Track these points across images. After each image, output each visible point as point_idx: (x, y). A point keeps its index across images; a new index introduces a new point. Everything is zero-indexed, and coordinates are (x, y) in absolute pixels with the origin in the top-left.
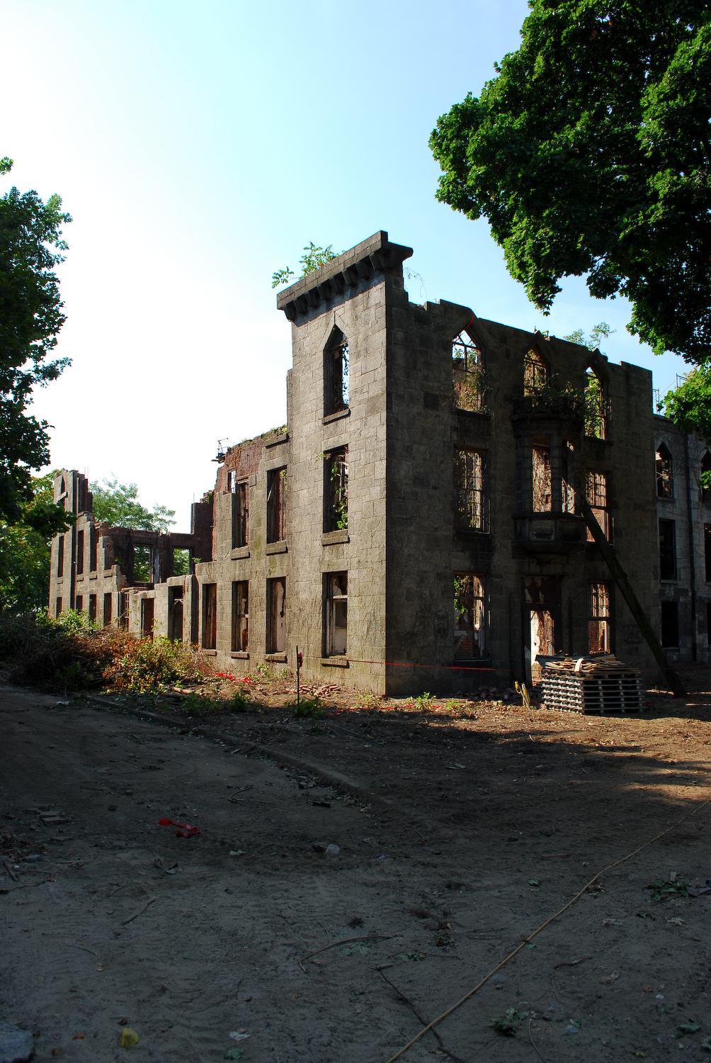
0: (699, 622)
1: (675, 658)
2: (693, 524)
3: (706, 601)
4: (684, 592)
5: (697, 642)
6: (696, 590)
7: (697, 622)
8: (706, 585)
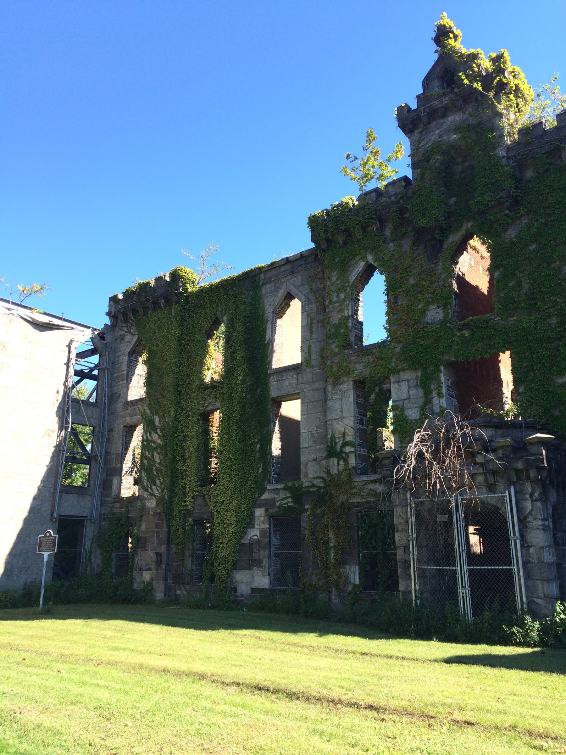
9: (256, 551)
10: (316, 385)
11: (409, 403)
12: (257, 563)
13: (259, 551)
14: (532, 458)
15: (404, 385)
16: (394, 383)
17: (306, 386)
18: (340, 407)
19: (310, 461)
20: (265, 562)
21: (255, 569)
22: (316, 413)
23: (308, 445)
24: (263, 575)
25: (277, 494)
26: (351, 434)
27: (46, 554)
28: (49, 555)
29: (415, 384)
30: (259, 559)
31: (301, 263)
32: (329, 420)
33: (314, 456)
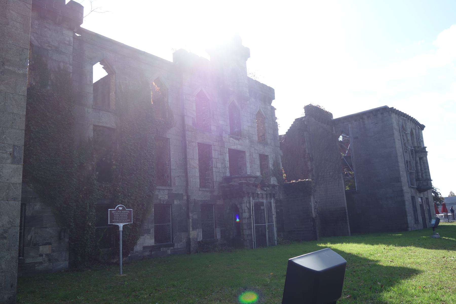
0: (192, 220)
1: (169, 252)
2: (187, 142)
5: (191, 237)
6: (189, 194)
7: (191, 220)
8: (199, 190)
9: (146, 224)
12: (148, 232)
14: (276, 191)
16: (213, 150)
20: (152, 231)
21: (146, 235)
23: (175, 168)
24: (151, 238)
27: (121, 225)
28: (124, 226)
30: (148, 229)
32: (188, 158)
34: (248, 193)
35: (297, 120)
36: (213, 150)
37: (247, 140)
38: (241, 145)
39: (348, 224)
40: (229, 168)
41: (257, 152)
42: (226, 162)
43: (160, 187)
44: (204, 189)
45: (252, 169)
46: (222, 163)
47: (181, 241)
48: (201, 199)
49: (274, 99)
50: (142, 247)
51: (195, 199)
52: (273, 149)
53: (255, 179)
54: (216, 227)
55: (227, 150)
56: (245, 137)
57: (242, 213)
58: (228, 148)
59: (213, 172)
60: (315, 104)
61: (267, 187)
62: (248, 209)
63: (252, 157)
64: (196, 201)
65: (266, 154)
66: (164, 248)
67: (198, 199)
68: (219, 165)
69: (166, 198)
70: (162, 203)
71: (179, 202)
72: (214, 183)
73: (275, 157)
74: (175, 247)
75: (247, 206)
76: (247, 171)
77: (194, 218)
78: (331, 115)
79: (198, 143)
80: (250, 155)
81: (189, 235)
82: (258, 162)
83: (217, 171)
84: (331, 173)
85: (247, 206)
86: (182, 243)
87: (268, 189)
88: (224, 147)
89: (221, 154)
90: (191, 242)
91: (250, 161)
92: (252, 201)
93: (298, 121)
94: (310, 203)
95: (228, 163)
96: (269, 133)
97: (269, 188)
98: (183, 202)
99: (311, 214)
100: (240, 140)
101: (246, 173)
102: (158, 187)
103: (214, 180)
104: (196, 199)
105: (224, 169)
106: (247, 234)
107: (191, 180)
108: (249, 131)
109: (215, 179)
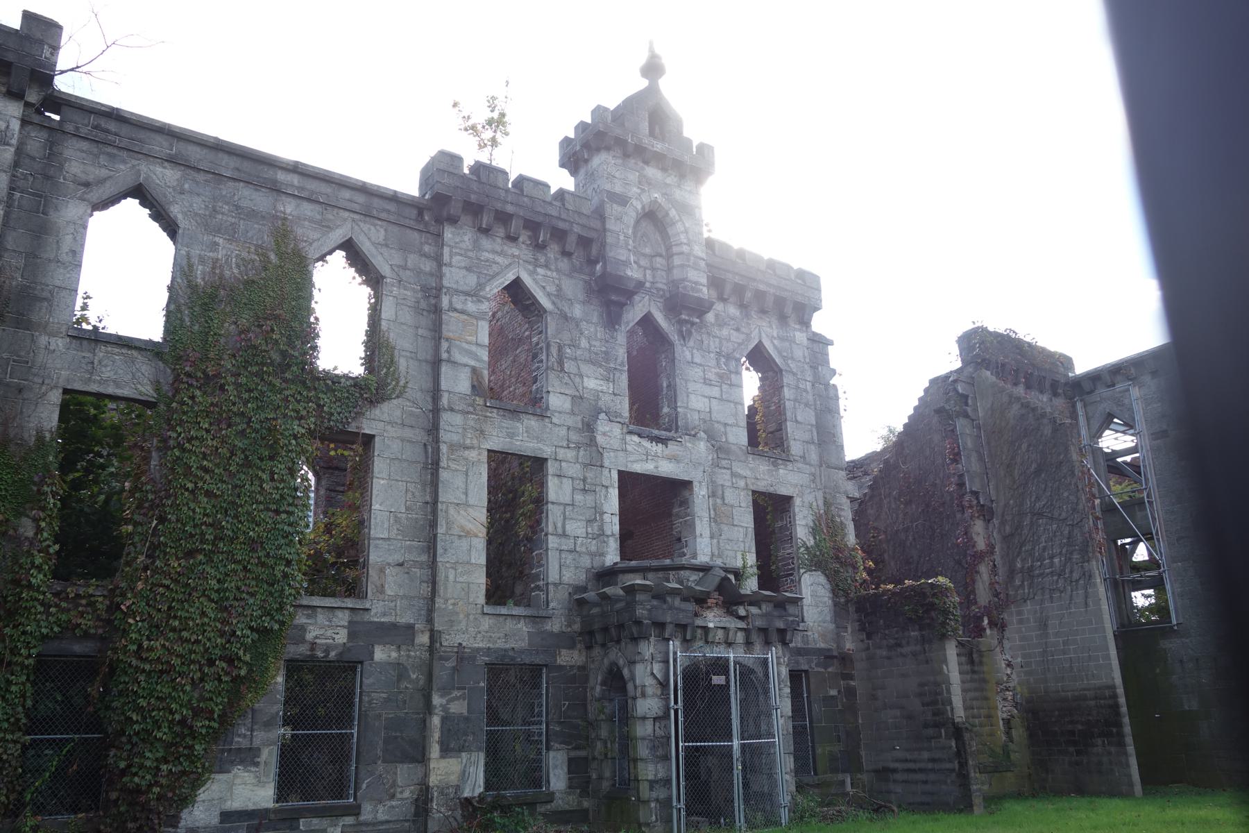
0: (444, 720)
2: (444, 448)
3: (483, 659)
4: (398, 633)
5: (433, 780)
6: (437, 627)
7: (436, 721)
10: (408, 433)
11: (572, 510)
12: (249, 757)
13: (252, 731)
14: (791, 619)
15: (567, 485)
16: (553, 475)
17: (389, 428)
18: (464, 486)
19: (389, 564)
20: (269, 756)
22: (407, 482)
23: (386, 536)
24: (259, 781)
25: (309, 617)
26: (480, 535)
29: (582, 487)
30: (250, 748)
31: (388, 207)
33: (398, 557)
34: (661, 626)
35: (934, 382)
36: (553, 475)
37: (702, 443)
38: (673, 458)
39: (1131, 749)
40: (618, 536)
41: (742, 483)
42: (607, 518)
43: (316, 601)
44: (504, 610)
45: (718, 542)
46: (589, 521)
47: (393, 797)
48: (491, 646)
49: (817, 309)
50: (217, 813)
51: (460, 644)
52: (813, 475)
53: (701, 574)
54: (548, 749)
55: (615, 476)
56: (693, 433)
57: (635, 698)
58: (620, 473)
59: (547, 549)
60: (997, 325)
61: (751, 604)
62: (660, 683)
63: (719, 501)
64: (466, 650)
65: (784, 491)
66: (315, 821)
67: (476, 645)
68: (576, 528)
69: (342, 637)
70: (320, 654)
71: (394, 655)
72: (551, 588)
73: (821, 503)
74: (366, 816)
75: (652, 674)
76: (698, 548)
77: (451, 711)
78: (1067, 362)
79: (489, 451)
80: (713, 495)
81: (426, 775)
82: (746, 520)
83: (564, 547)
84: (1056, 560)
85: (655, 672)
86: (394, 803)
87: (754, 610)
88: (602, 466)
89: (584, 490)
90: (432, 797)
91: (712, 516)
92: (675, 653)
93: (941, 385)
94: (945, 667)
95: (616, 520)
96: (797, 421)
97: (760, 609)
98: (412, 654)
99: (948, 708)
100: (670, 442)
101: (695, 556)
102: (305, 601)
103: (551, 580)
104: (464, 644)
105: (594, 542)
106: (651, 777)
107: (451, 577)
108: (710, 412)
109: (553, 576)
